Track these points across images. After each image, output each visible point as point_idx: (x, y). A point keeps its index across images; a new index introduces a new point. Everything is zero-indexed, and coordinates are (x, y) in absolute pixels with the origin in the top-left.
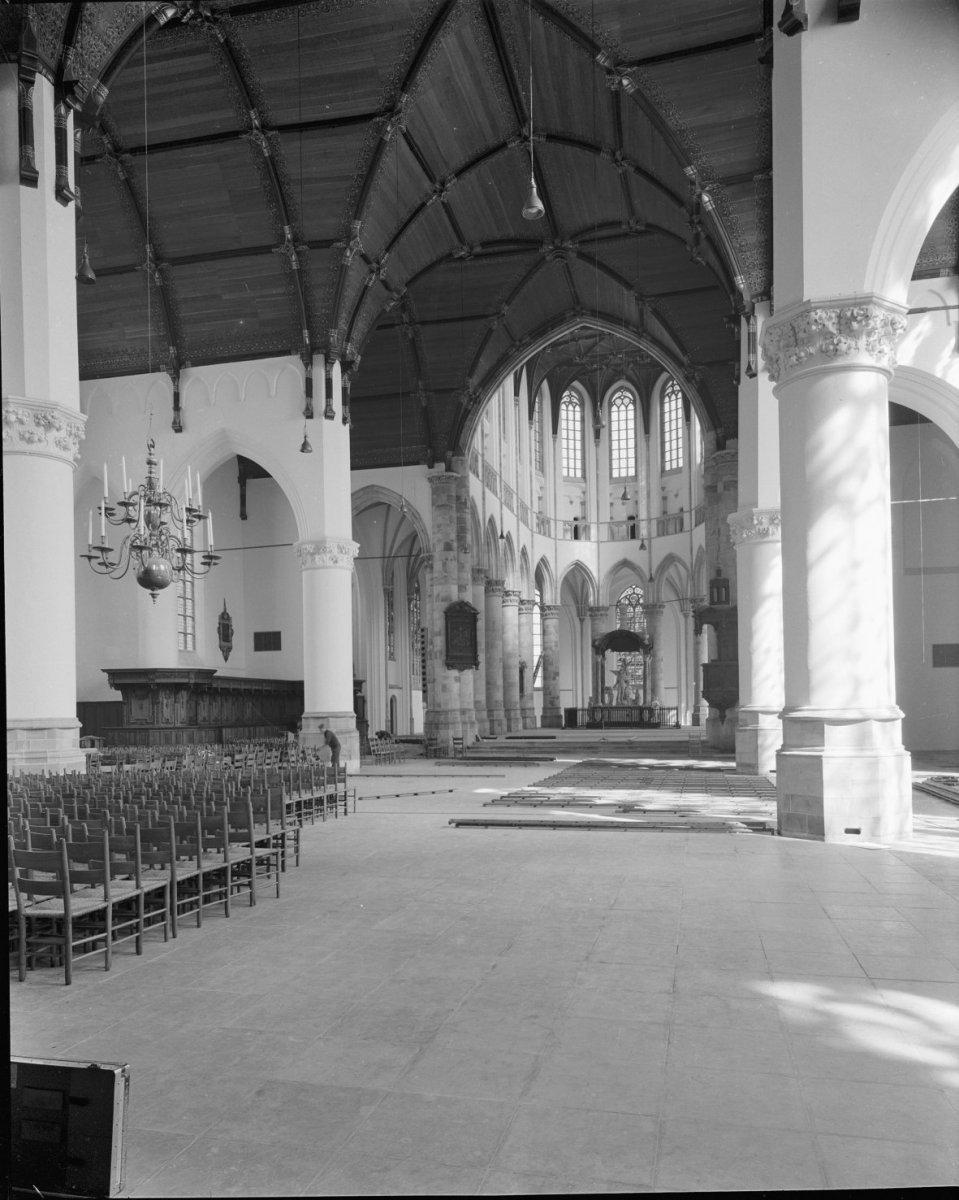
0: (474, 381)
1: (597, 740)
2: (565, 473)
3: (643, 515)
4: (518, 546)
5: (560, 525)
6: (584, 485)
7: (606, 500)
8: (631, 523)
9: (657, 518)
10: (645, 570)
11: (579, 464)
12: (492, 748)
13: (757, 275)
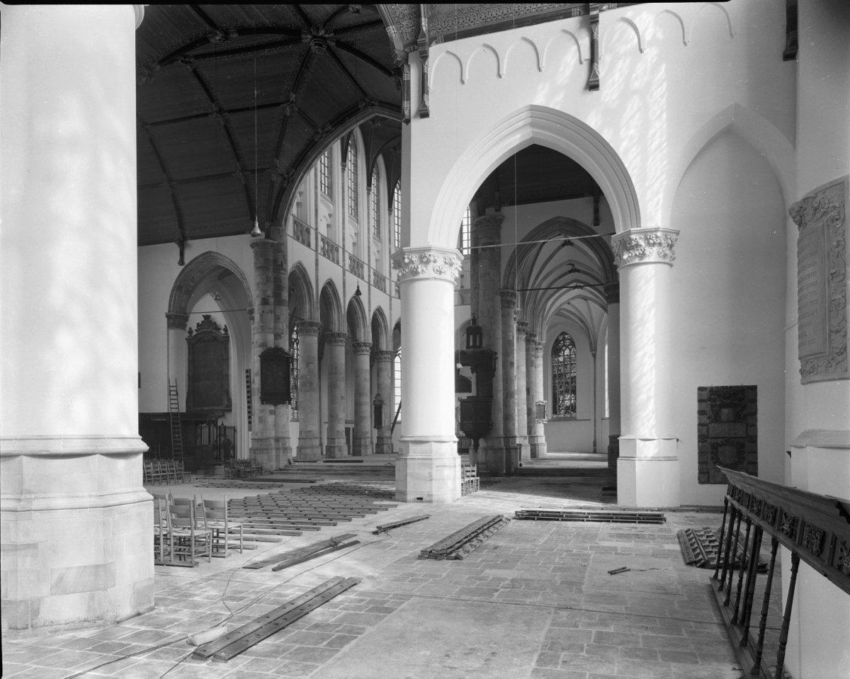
0: (283, 163)
1: (383, 464)
4: (370, 311)
12: (298, 470)
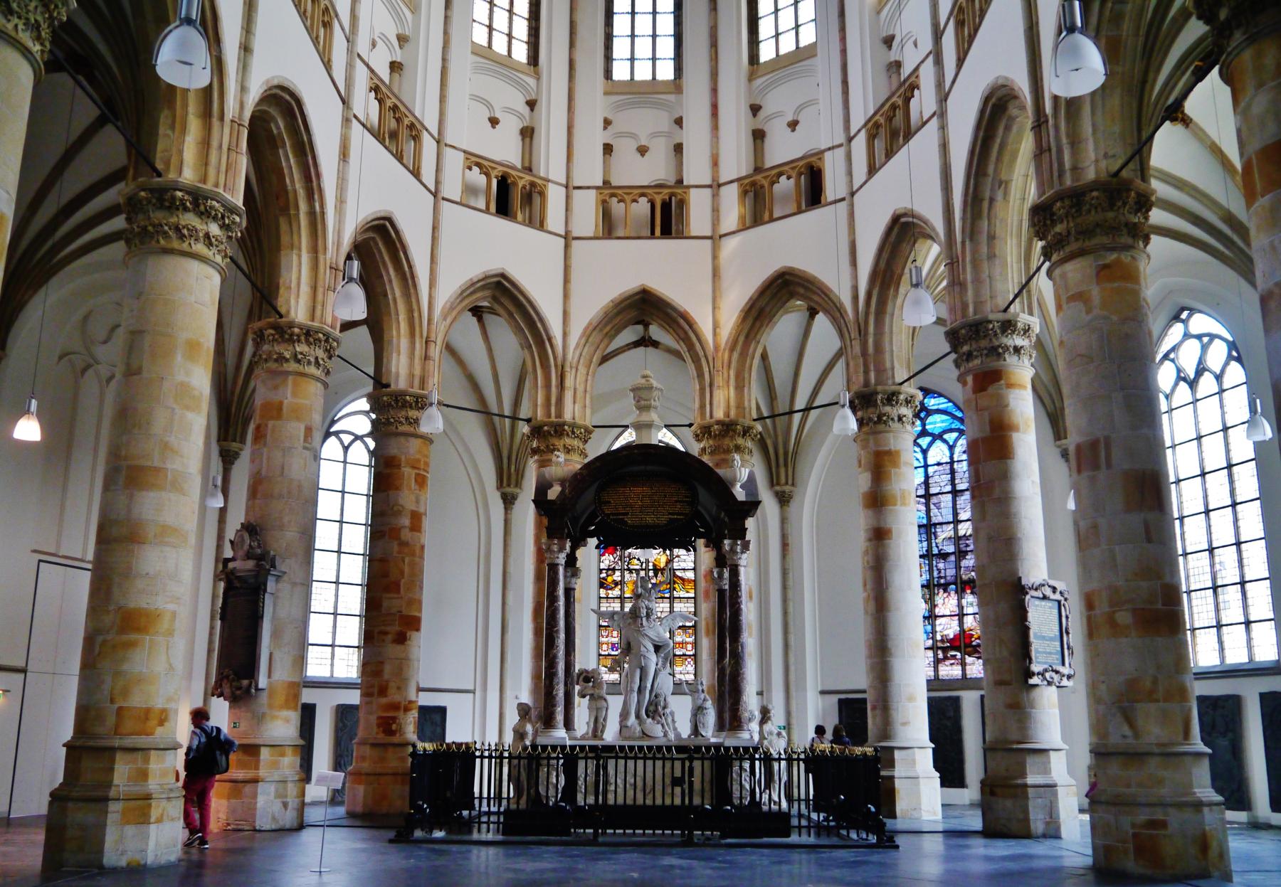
2: (480, 36)
3: (697, 170)
5: (454, 161)
6: (531, 81)
9: (738, 180)
11: (521, 29)
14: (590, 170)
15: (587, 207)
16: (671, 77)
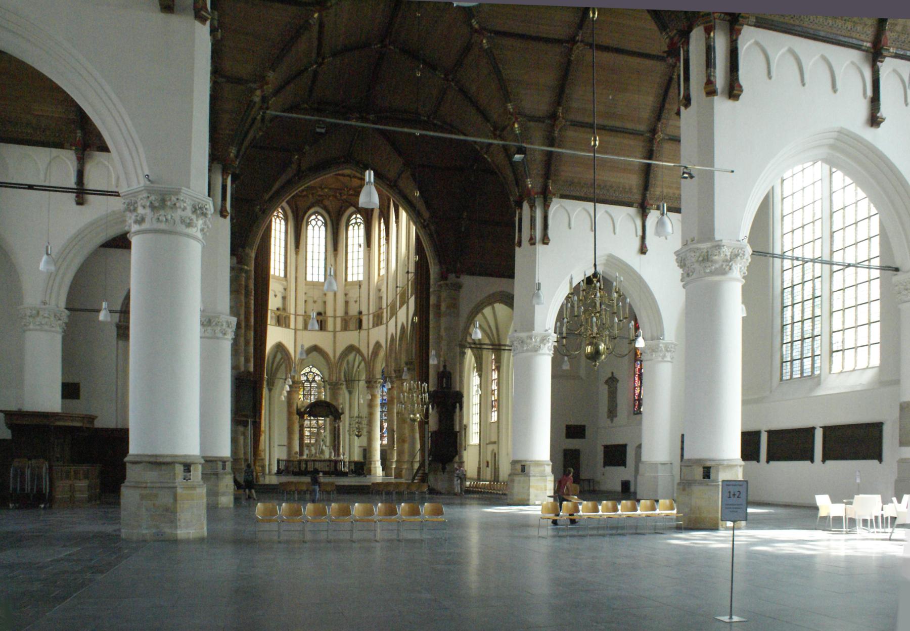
3: (330, 312)
6: (285, 283)
7: (301, 298)
8: (320, 318)
9: (341, 317)
10: (331, 355)
13: (539, 181)
14: (301, 311)
15: (300, 320)
16: (323, 281)
